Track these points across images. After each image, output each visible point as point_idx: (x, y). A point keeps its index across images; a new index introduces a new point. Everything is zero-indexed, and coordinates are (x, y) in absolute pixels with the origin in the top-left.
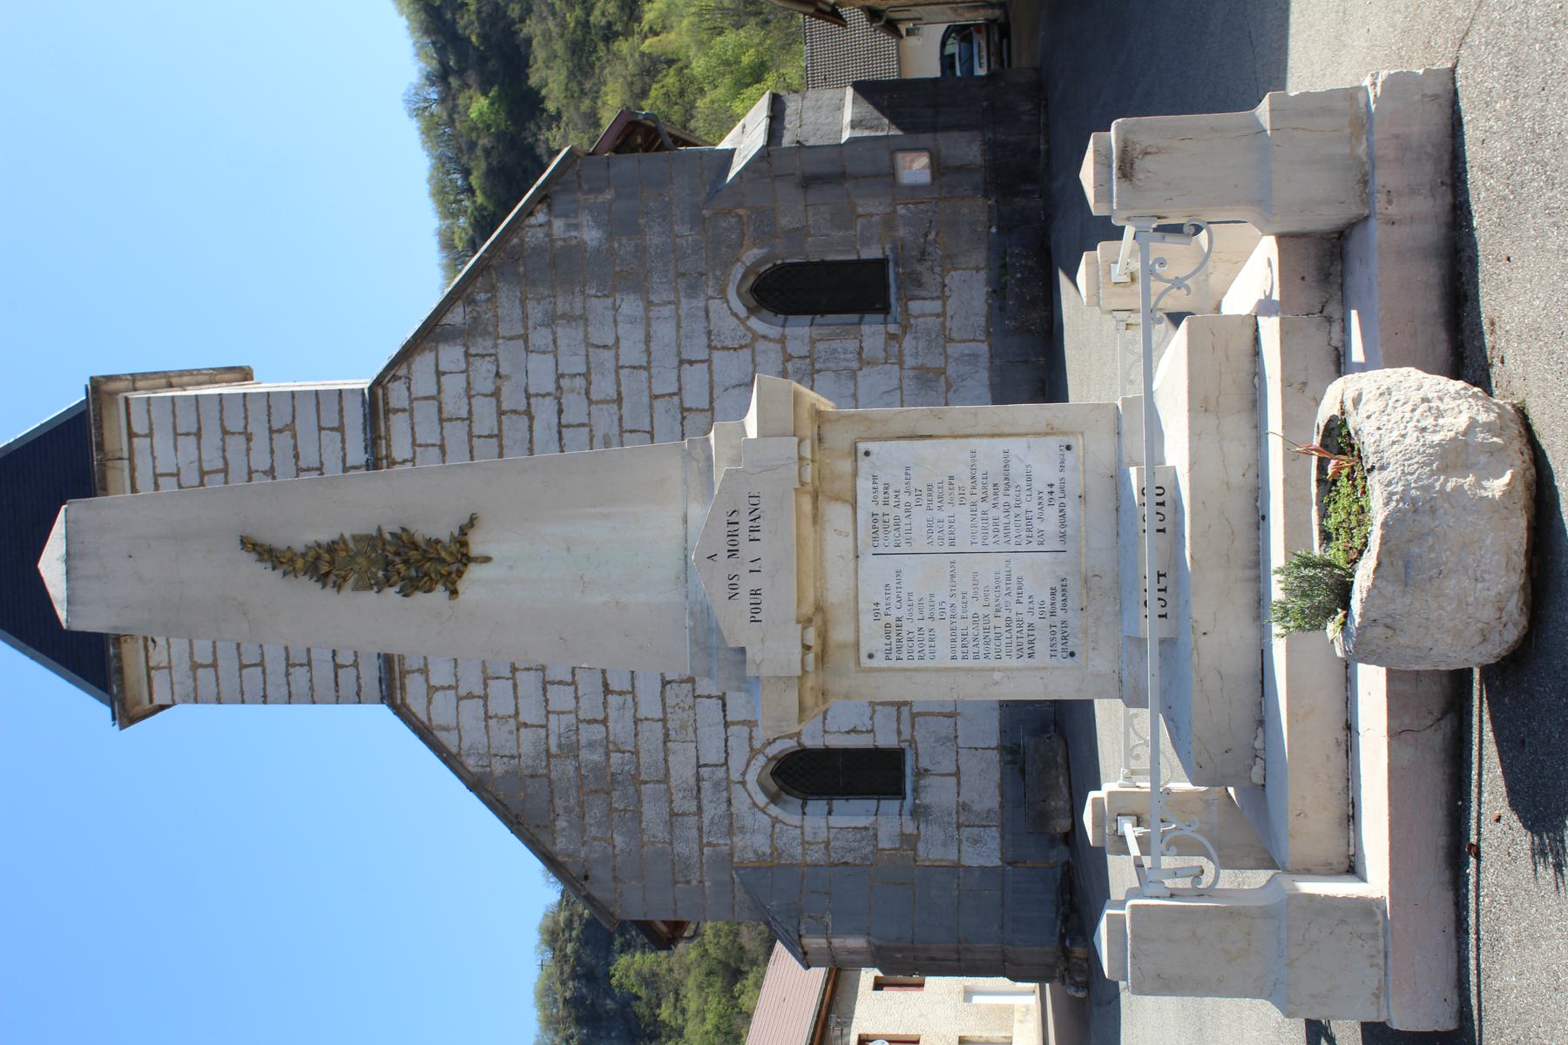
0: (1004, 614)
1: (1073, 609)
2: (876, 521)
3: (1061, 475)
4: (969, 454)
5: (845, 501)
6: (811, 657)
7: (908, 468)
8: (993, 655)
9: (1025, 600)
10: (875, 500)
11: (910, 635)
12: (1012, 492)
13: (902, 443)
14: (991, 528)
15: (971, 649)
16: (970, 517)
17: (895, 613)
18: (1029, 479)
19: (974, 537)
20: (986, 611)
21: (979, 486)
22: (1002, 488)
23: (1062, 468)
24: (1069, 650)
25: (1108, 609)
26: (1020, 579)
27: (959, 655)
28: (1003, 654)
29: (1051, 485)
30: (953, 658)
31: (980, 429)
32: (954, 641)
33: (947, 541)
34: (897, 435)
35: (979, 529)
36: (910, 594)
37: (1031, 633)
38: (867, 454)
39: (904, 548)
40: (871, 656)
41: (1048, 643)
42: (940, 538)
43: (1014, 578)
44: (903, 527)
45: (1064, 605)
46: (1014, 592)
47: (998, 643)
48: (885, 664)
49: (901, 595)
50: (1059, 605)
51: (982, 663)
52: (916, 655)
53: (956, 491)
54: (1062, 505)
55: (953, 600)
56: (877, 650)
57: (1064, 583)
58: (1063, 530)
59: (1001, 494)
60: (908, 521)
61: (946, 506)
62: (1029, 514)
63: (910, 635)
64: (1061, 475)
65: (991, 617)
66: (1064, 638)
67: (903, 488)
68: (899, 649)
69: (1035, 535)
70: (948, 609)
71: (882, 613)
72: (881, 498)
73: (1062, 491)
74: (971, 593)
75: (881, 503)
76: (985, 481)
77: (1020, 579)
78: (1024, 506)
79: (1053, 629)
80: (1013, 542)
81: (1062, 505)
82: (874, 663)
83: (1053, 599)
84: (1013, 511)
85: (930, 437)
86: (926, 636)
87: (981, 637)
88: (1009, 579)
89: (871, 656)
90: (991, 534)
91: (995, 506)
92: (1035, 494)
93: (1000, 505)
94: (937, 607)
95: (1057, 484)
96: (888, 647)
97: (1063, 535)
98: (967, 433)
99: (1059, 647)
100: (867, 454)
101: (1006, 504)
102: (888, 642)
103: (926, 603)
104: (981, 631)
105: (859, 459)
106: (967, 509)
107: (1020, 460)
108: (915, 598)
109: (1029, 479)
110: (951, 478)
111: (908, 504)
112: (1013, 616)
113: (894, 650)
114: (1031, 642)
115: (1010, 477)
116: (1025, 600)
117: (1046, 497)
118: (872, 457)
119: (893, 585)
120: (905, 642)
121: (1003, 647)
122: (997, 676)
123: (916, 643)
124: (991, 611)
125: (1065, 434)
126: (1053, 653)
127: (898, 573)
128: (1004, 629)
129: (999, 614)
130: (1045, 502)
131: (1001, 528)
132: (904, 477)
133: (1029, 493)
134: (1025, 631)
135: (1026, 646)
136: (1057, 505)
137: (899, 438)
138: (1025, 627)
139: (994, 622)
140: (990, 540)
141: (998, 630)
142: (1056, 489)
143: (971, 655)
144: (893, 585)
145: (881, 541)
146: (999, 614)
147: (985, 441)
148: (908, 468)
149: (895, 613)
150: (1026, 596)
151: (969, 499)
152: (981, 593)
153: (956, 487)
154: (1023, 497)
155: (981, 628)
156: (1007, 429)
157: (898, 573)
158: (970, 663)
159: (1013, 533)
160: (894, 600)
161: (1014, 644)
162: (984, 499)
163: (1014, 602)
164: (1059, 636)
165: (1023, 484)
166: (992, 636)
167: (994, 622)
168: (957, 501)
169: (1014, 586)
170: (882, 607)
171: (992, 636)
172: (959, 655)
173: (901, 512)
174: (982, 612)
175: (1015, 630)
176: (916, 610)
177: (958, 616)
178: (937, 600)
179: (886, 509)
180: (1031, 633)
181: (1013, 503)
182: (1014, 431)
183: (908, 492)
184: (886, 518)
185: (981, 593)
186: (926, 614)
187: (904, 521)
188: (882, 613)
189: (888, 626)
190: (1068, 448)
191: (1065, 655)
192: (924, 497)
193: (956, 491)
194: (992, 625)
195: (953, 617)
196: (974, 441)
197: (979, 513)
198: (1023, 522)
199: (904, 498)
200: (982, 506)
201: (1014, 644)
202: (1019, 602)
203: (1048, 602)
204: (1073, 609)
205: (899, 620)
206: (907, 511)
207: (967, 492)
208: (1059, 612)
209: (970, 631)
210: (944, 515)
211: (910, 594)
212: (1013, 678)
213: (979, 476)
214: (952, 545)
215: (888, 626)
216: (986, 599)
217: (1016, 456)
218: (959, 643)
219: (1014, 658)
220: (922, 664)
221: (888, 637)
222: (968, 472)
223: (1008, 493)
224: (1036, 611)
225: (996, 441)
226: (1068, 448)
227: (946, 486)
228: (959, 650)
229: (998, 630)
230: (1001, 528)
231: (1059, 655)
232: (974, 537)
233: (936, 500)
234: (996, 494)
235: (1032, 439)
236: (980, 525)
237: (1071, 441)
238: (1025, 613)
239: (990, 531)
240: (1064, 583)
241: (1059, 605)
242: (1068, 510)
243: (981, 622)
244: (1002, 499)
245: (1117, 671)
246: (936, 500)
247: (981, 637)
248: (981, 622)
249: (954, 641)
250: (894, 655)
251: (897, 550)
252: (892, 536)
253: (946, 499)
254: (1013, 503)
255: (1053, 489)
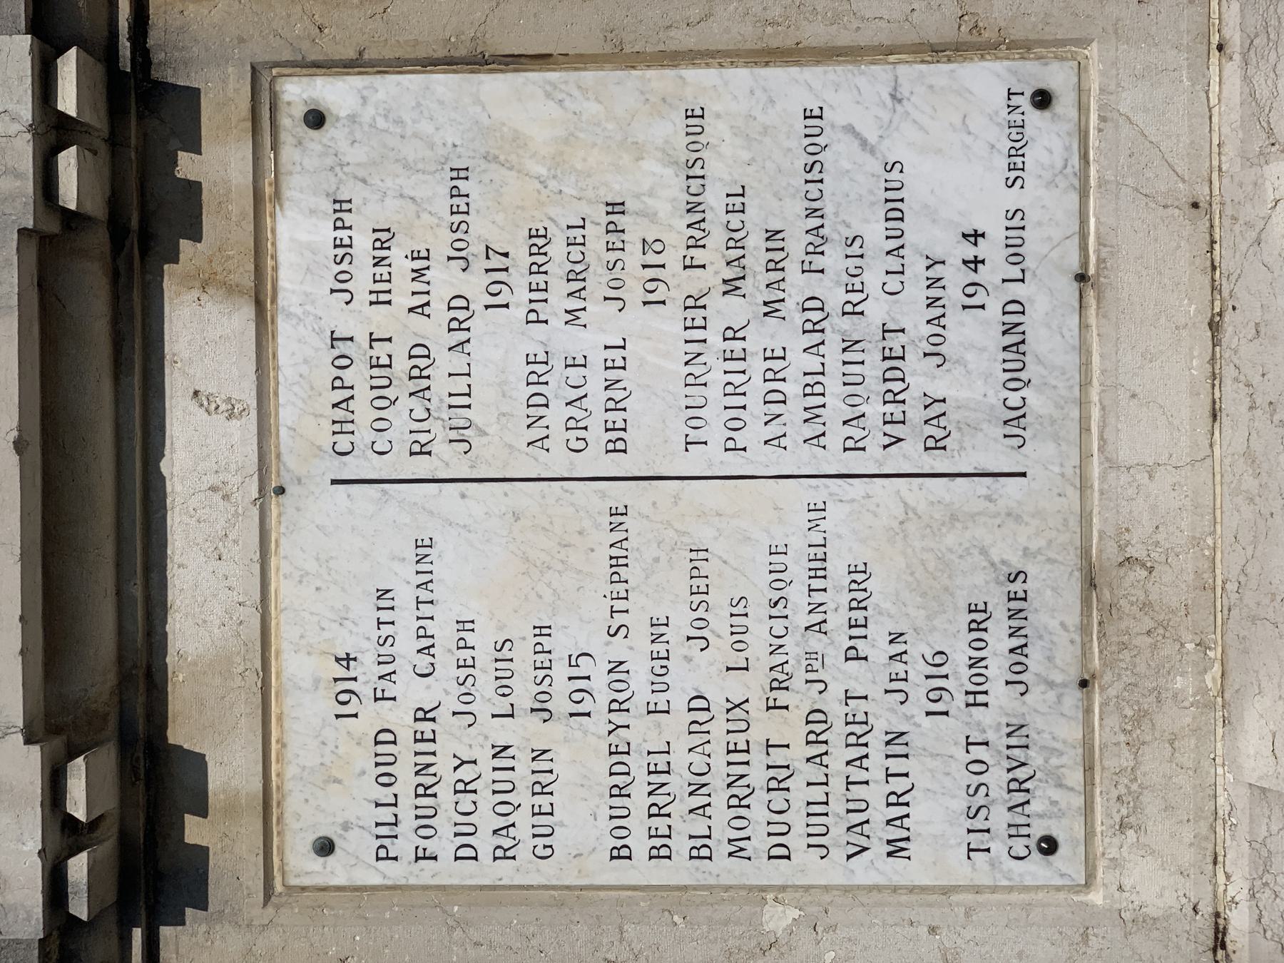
0: (800, 699)
1: (1051, 685)
2: (342, 362)
3: (1012, 199)
4: (681, 121)
5: (231, 290)
6: (78, 867)
7: (460, 173)
8: (759, 843)
9: (877, 647)
10: (341, 286)
11: (466, 773)
12: (833, 259)
13: (443, 83)
14: (757, 388)
15: (684, 827)
16: (680, 351)
17: (412, 692)
18: (895, 213)
19: (695, 422)
20: (736, 687)
21: (717, 238)
22: (796, 245)
23: (1015, 176)
24: (1038, 830)
25: (1179, 682)
26: (859, 572)
27: (640, 844)
28: (796, 841)
29: (975, 237)
30: (620, 854)
31: (717, 34)
32: (619, 792)
33: (597, 435)
34: (421, 53)
35: (714, 392)
36: (464, 625)
37: (896, 765)
38: (316, 119)
39: (446, 459)
40: (325, 847)
41: (960, 803)
42: (572, 425)
43: (837, 568)
44: (441, 385)
45: (1019, 668)
46: (837, 621)
47: (778, 801)
48: (371, 876)
49: (431, 628)
50: (997, 668)
51: (723, 869)
52: (485, 843)
53: (633, 257)
54: (1015, 307)
55: (618, 650)
56: (346, 826)
57: (1017, 587)
58: (1014, 399)
59: (792, 268)
60: (457, 362)
61: (596, 309)
62: (895, 342)
63: (466, 773)
64: (1012, 199)
65: (756, 707)
66: (1018, 786)
67: (441, 246)
68: (425, 821)
69: (916, 414)
70: (600, 682)
71: (366, 691)
72: (362, 283)
73: (1015, 254)
74: (681, 622)
75: (362, 297)
76: (735, 221)
77: (859, 572)
78: (877, 310)
79: (978, 752)
80: (835, 439)
81: (1015, 307)
82: (335, 871)
83: (979, 644)
84: (838, 326)
85: (542, 60)
86: (523, 772)
87: (718, 780)
88: (818, 569)
89: (325, 847)
90: (756, 407)
91: (771, 309)
92: (916, 267)
93: (790, 308)
94: (560, 672)
95: (996, 230)
96: (386, 815)
97: (1016, 418)
98: (672, 46)
99: (999, 818)
100: (316, 119)
101: (812, 303)
102: (385, 795)
103: (523, 656)
104: (719, 760)
105: (285, 137)
106: (669, 321)
107: (864, 143)
108: (483, 641)
109: (895, 213)
110: (615, 208)
111: (459, 303)
112: (836, 711)
113: (408, 822)
114: (897, 800)
115: (829, 210)
116: (877, 647)
117: (955, 277)
118: (329, 131)
119: (405, 596)
120: (445, 793)
121: (797, 818)
122: (778, 918)
123: (486, 800)
124: (753, 687)
125: (1023, 48)
126: (976, 841)
127: (423, 549)
128: (800, 751)
129: (782, 697)
130: (953, 294)
131: (792, 389)
132: (443, 204)
133: (893, 263)
134: (877, 761)
135: (879, 813)
136: (994, 307)
137: (429, 64)
138: (876, 742)
139: (764, 727)
140: (753, 434)
141: (778, 757)
142: (992, 249)
143: (681, 845)
144: (405, 596)
145: (364, 436)
146: (782, 697)
147: (741, 76)
148: (460, 173)
149: (412, 692)
150: (878, 633)
151: (681, 284)
152: (720, 622)
153: (633, 238)
154: (873, 279)
155: (718, 749)
156: (815, 33)
157: (423, 549)
158: (678, 871)
159: (835, 408)
160: (406, 645)
161: (838, 806)
162: (732, 287)
163: (835, 657)
164: (997, 778)
165: (875, 232)
166: (758, 775)
167: (764, 727)
168: (634, 293)
169: (837, 600)
170: (367, 670)
171: (758, 775)
172: (640, 844)
173: (434, 330)
174: (720, 691)
175: (839, 756)
176: (485, 684)
177: (638, 705)
178: (561, 645)
179: (381, 320)
180: (896, 765)
181: (836, 298)
182: (844, 39)
183: (460, 257)
184: (381, 350)
185: (720, 622)
186: (524, 694)
187: (445, 362)
188: (366, 691)
189: (386, 736)
190: (1043, 99)
191: (1019, 847)
192: (519, 278)
193: (633, 257)
194: (757, 735)
195: (618, 707)
196: (692, 75)
197: (714, 337)
198: (873, 367)
199: (445, 280)
200: (725, 310)
201: (838, 806)
202: (853, 656)
203: (960, 655)
204: (1051, 685)
205: (424, 715)
206: (456, 326)
207: (672, 259)
208: (998, 693)
209: (680, 758)
210: (588, 342)
211: (464, 625)
212: (833, 928)
213: (715, 200)
214: (616, 448)
215: (386, 736)
216: (739, 645)
217: (850, 129)
218: (639, 800)
219: (838, 855)
220: (505, 873)
221: (386, 780)
222: (673, 188)
223: (819, 262)
224: (918, 689)
225: (776, 75)
226: (1043, 99)
227: (596, 238)
228: (638, 825)
229: (778, 757)
230: (792, 389)
231: (998, 847)
232: (695, 422)
233: (558, 289)
234: (774, 266)
235: (910, 73)
236: (717, 378)
237: (1057, 77)
238: (876, 692)
239: (754, 400)
240: (1017, 587)
241: (997, 668)
242: (1034, 326)
243: (718, 728)
244: (797, 286)
245: (1206, 909)
246: (558, 289)
247: (718, 780)
248: (718, 728)
249: (619, 792)
250: (404, 846)
251: (422, 467)
252: (399, 419)
253: (597, 282)
254: (836, 298)
255: (983, 250)
